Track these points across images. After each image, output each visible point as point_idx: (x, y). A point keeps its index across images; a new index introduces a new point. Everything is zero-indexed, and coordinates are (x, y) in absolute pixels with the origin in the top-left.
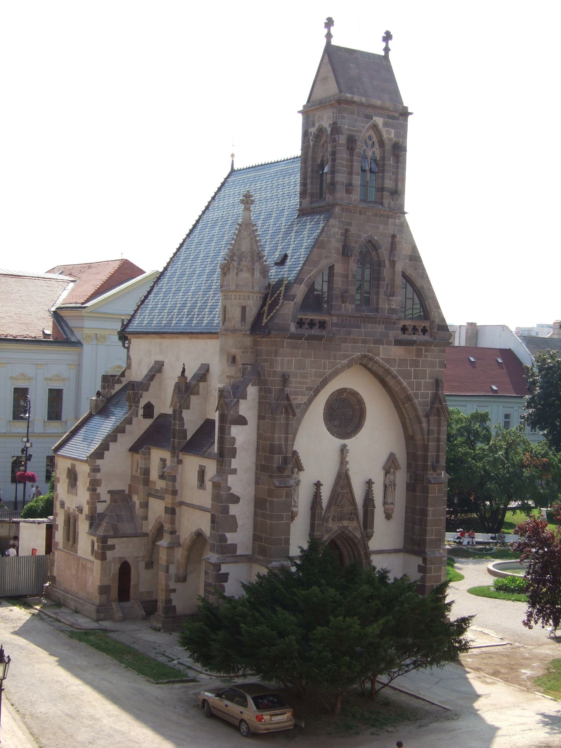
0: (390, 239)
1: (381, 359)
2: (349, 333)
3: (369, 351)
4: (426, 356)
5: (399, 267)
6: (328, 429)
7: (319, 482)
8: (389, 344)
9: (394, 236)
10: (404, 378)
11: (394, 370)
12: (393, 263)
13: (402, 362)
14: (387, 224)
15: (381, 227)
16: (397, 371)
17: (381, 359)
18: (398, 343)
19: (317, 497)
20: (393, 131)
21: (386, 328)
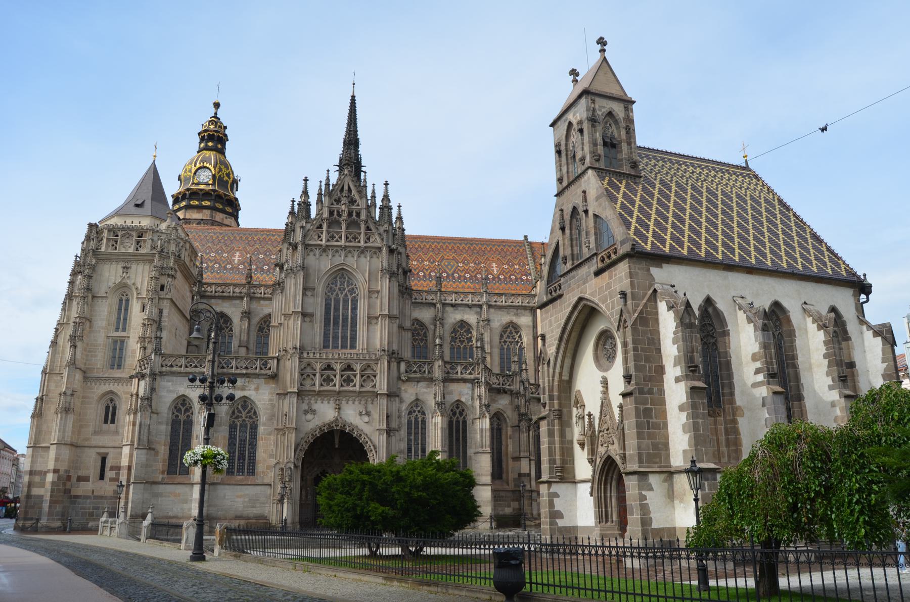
0: (582, 194)
2: (570, 285)
4: (615, 275)
5: (591, 213)
7: (590, 412)
8: (591, 279)
9: (584, 192)
10: (603, 304)
11: (596, 300)
12: (586, 212)
16: (599, 299)
18: (598, 273)
19: (591, 424)
20: (578, 115)
21: (589, 268)
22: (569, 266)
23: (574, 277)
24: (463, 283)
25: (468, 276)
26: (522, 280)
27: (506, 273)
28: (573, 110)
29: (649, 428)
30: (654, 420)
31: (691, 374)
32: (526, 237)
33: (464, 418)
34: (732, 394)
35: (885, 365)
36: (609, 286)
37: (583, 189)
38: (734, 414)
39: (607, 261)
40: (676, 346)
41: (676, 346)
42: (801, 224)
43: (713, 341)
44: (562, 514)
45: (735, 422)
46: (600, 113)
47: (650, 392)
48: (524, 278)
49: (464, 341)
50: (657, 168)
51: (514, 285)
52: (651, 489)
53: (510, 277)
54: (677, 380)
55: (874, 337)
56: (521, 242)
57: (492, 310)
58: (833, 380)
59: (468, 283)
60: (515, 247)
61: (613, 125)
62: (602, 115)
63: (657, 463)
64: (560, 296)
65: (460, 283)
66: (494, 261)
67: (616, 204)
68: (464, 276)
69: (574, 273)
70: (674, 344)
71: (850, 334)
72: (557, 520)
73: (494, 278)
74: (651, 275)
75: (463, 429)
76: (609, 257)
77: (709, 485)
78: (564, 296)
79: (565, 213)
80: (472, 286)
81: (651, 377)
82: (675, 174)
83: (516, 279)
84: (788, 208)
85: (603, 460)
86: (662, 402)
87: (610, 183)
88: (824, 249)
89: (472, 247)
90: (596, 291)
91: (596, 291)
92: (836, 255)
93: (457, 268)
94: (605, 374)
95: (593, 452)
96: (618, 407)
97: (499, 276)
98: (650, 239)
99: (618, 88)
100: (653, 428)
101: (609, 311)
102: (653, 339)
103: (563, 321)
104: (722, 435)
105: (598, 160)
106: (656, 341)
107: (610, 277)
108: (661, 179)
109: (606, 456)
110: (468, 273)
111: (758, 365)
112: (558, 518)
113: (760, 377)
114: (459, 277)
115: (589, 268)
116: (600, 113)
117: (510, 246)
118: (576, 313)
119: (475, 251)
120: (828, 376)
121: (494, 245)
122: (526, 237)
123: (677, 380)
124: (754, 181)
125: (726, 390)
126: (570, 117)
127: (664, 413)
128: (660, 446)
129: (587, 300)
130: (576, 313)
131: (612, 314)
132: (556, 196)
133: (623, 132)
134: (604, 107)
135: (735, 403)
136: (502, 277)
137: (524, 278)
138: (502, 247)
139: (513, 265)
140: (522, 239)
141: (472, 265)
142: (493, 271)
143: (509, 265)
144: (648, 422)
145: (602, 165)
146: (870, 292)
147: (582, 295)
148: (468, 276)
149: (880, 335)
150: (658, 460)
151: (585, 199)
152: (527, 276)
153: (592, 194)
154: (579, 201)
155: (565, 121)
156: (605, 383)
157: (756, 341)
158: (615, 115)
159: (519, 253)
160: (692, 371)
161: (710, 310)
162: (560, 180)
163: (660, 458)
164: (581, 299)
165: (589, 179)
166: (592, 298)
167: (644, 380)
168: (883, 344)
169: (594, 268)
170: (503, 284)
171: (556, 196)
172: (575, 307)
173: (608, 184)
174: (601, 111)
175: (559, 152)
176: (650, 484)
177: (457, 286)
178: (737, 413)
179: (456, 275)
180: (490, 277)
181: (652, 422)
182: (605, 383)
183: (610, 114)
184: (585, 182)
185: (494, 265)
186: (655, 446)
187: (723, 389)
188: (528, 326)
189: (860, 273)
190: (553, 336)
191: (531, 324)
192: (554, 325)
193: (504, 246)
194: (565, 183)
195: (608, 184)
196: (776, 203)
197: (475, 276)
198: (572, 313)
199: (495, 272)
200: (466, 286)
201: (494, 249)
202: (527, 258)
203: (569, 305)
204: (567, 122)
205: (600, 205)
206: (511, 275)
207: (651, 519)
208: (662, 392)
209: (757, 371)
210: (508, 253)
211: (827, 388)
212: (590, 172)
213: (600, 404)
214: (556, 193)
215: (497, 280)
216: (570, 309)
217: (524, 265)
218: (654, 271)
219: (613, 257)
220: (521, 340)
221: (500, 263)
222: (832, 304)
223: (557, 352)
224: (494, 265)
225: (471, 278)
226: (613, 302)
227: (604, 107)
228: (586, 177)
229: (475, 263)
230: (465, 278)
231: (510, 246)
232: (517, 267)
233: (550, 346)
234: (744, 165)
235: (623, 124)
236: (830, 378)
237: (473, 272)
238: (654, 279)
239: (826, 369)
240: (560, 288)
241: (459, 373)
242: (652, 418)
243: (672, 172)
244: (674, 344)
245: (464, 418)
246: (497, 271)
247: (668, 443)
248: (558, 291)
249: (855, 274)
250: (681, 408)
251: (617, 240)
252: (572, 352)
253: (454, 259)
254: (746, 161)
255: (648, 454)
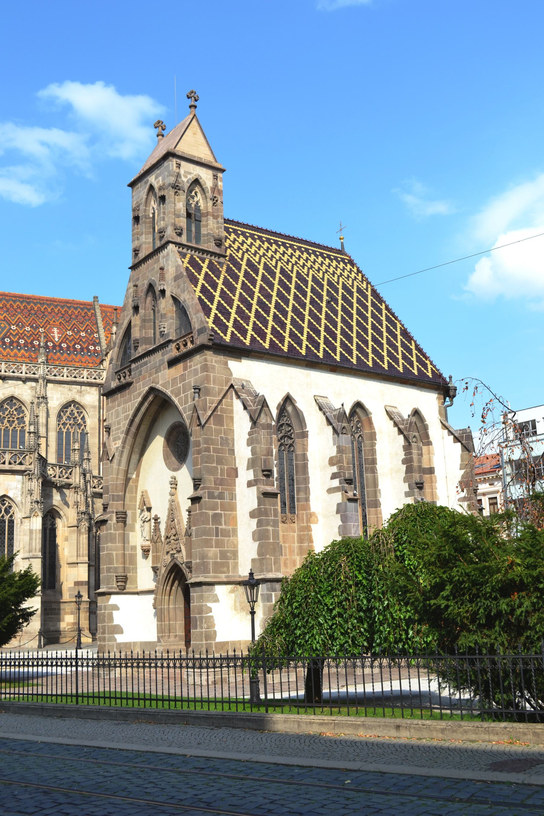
1: (161, 385)
3: (153, 382)
4: (190, 367)
5: (168, 294)
6: (166, 464)
7: (156, 516)
8: (164, 369)
9: (162, 269)
10: (176, 397)
11: (168, 392)
13: (174, 380)
14: (159, 261)
15: (156, 266)
16: (172, 392)
17: (161, 385)
18: (172, 363)
20: (160, 178)
22: (141, 350)
23: (146, 364)
24: (15, 350)
25: (22, 342)
26: (89, 350)
27: (70, 341)
28: (157, 172)
29: (217, 535)
30: (223, 527)
31: (265, 478)
32: (96, 298)
33: (11, 516)
34: (307, 499)
35: (462, 472)
36: (183, 378)
37: (162, 265)
38: (308, 521)
39: (183, 350)
40: (250, 448)
41: (250, 448)
42: (392, 319)
43: (290, 442)
44: (122, 629)
45: (309, 529)
46: (185, 180)
47: (221, 496)
48: (92, 348)
49: (13, 421)
50: (245, 246)
51: (79, 356)
52: (217, 600)
53: (74, 345)
54: (250, 484)
55: (454, 442)
56: (89, 304)
57: (50, 385)
58: (410, 487)
59: (23, 351)
60: (82, 309)
61: (199, 195)
62: (187, 182)
63: (224, 573)
64: (128, 385)
65: (12, 350)
66: (55, 326)
67: (196, 287)
68: (18, 342)
69: (146, 359)
70: (248, 445)
71: (431, 439)
72: (116, 636)
73: (54, 347)
74: (229, 369)
75: (9, 530)
76: (185, 345)
77: (276, 596)
78: (134, 384)
79: (140, 289)
80: (27, 355)
81: (222, 479)
82: (264, 255)
83: (82, 349)
84: (381, 301)
85: (169, 568)
86: (232, 508)
87: (192, 262)
88: (413, 347)
89: (29, 307)
90: (169, 381)
91: (169, 381)
92: (424, 355)
93: (8, 331)
94: (174, 474)
95: (156, 559)
96: (187, 510)
97: (61, 344)
98: (231, 329)
99: (209, 152)
100: (222, 536)
101: (182, 406)
102: (227, 439)
103: (131, 413)
104: (294, 543)
105: (180, 235)
106: (230, 442)
107: (185, 369)
108: (248, 260)
109: (172, 564)
110: (23, 338)
111: (335, 469)
112: (116, 633)
113: (336, 483)
114: (12, 343)
115: (163, 355)
116: (185, 180)
117: (76, 309)
118: (146, 404)
119: (33, 312)
120: (405, 482)
121: (56, 306)
122: (96, 298)
123: (250, 484)
124: (349, 267)
125: (302, 495)
126: (152, 179)
127: (235, 518)
128: (229, 554)
129: (159, 391)
130: (146, 404)
131: (184, 409)
132: (130, 268)
133: (210, 203)
134: (190, 173)
135: (310, 509)
136: (64, 345)
137: (92, 348)
138: (66, 308)
139: (79, 331)
140: (90, 300)
141: (28, 329)
142: (54, 337)
143: (73, 330)
144: (217, 529)
145: (183, 239)
146: (454, 396)
147: (153, 385)
148: (22, 342)
149: (459, 441)
150: (225, 569)
151: (162, 277)
152: (95, 347)
153: (171, 272)
154: (155, 278)
155: (146, 183)
156: (174, 484)
157: (334, 445)
158: (202, 183)
159: (87, 318)
160: (265, 475)
161: (290, 409)
162: (136, 252)
163: (228, 567)
164: (152, 390)
165: (168, 254)
166: (164, 390)
167: (215, 484)
168: (462, 451)
169: (167, 358)
170: (65, 355)
171: (130, 268)
172: (145, 398)
173: (188, 263)
174: (186, 177)
175: (136, 219)
176: (216, 595)
177: (8, 354)
178: (312, 519)
179: (7, 340)
180: (50, 344)
181: (221, 529)
182: (174, 484)
183: (196, 182)
184: (164, 257)
185: (55, 330)
186: (223, 555)
187: (298, 494)
188: (94, 407)
189: (446, 375)
190: (119, 429)
191: (97, 404)
192: (122, 416)
193: (69, 308)
194: (142, 255)
195: (188, 263)
196: (369, 293)
197: (32, 343)
198: (141, 404)
199: (57, 339)
200: (20, 355)
201: (56, 310)
202: (97, 323)
203: (139, 394)
204: (148, 187)
205: (179, 286)
206: (75, 344)
207: (215, 632)
208: (233, 496)
209: (334, 476)
210: (73, 317)
211: (403, 495)
212: (171, 246)
213: (167, 506)
214: (131, 265)
215: (58, 349)
216: (140, 399)
217: (92, 333)
218: (233, 364)
219: (190, 346)
220: (85, 422)
221: (61, 327)
222: (416, 406)
223: (123, 447)
224: (55, 330)
225: (25, 345)
226: (186, 396)
227: (190, 173)
228: (165, 252)
229: (32, 327)
230: (19, 344)
231: (76, 309)
232: (83, 334)
233: (115, 440)
234: (339, 247)
235: (209, 194)
236: (407, 484)
237: (29, 337)
238: (231, 374)
239: (403, 475)
240: (130, 375)
241: (7, 463)
242: (221, 525)
243: (261, 252)
244: (248, 445)
245: (11, 516)
246: (59, 338)
247: (237, 551)
248: (127, 377)
249: (440, 375)
250: (253, 515)
251: (195, 328)
252: (140, 447)
253: (5, 319)
254: (342, 244)
255: (215, 563)
